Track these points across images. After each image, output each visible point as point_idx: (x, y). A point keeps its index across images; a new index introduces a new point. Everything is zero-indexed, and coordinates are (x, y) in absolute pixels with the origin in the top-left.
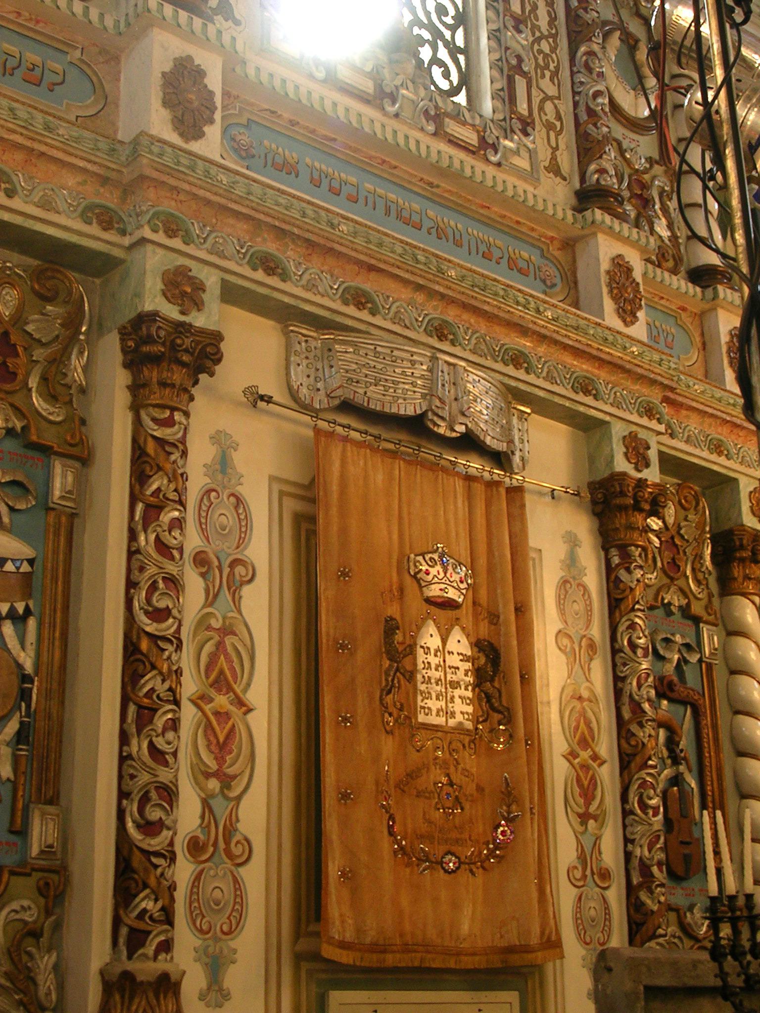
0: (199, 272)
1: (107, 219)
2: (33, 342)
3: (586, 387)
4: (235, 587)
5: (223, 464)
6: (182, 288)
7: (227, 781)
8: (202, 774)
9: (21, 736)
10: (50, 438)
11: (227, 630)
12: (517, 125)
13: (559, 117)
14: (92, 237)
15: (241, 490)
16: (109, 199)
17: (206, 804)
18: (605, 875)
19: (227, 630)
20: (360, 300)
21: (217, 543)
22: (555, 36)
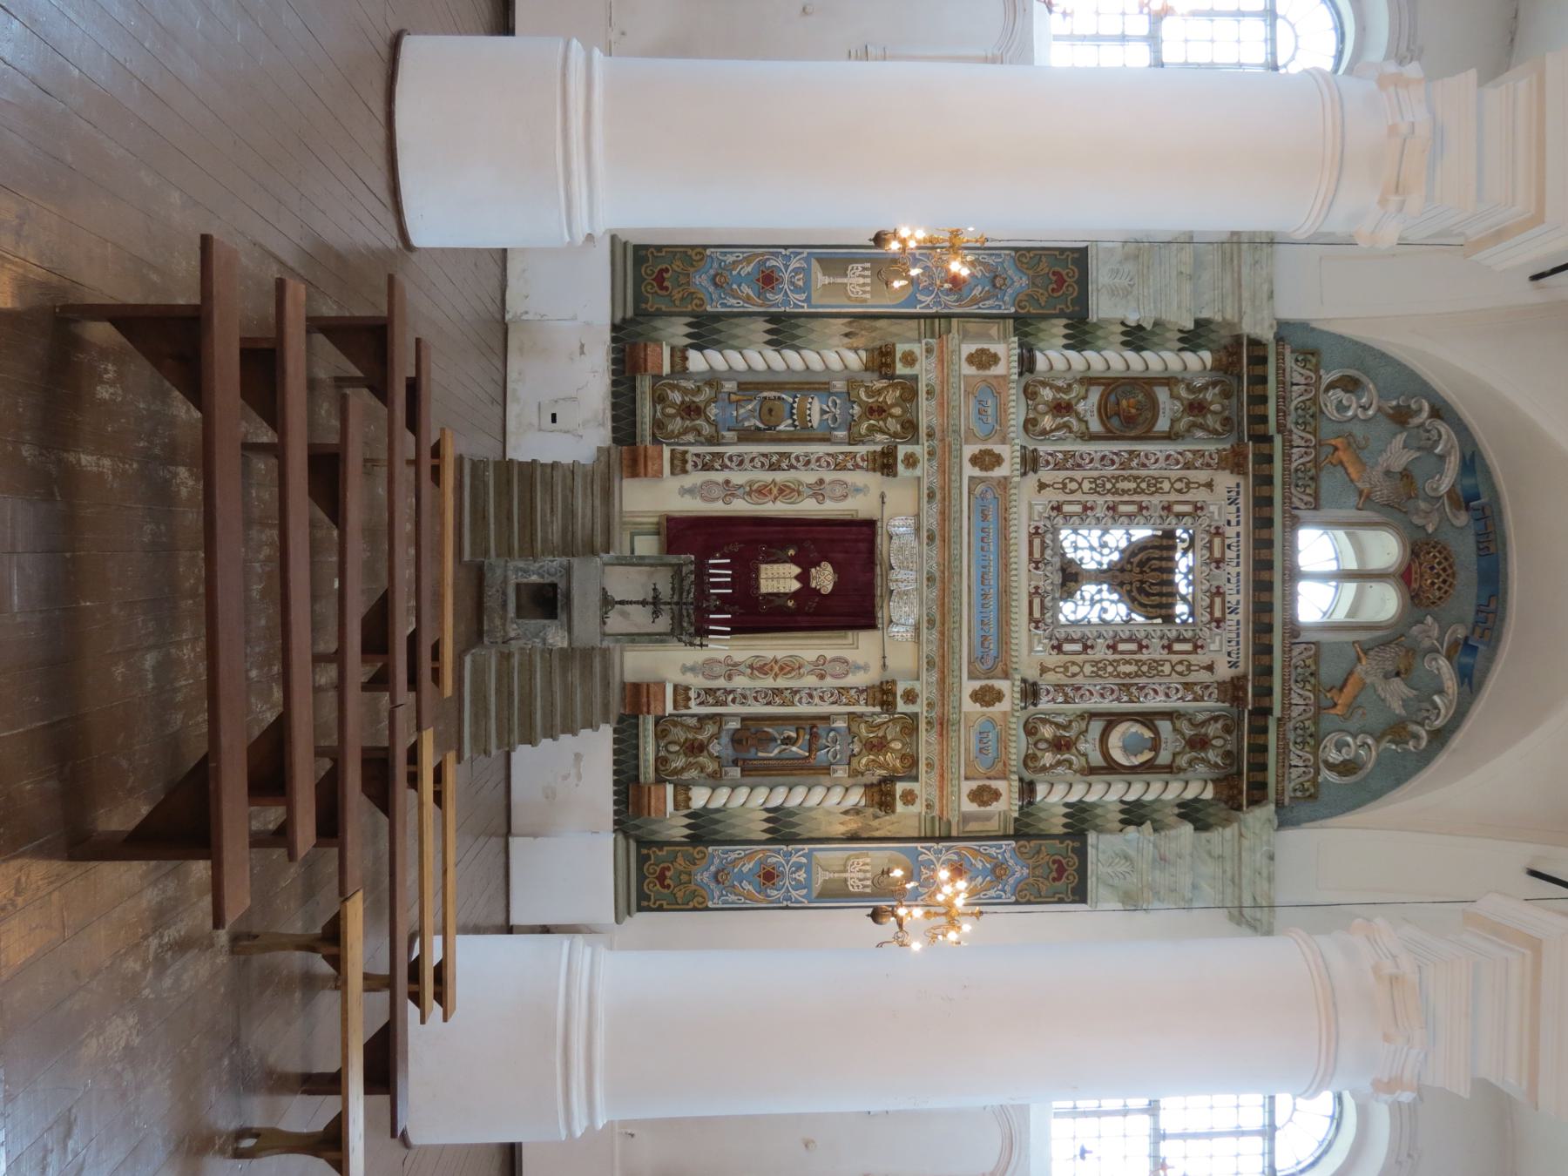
0: (920, 466)
1: (930, 436)
2: (885, 420)
3: (931, 664)
4: (815, 495)
5: (858, 490)
6: (911, 461)
7: (749, 494)
8: (751, 484)
9: (758, 429)
10: (854, 430)
11: (799, 493)
12: (1055, 643)
13: (1074, 675)
14: (923, 431)
15: (850, 499)
16: (938, 435)
17: (741, 486)
18: (730, 678)
19: (799, 493)
20: (931, 538)
21: (829, 488)
22: (1118, 676)
